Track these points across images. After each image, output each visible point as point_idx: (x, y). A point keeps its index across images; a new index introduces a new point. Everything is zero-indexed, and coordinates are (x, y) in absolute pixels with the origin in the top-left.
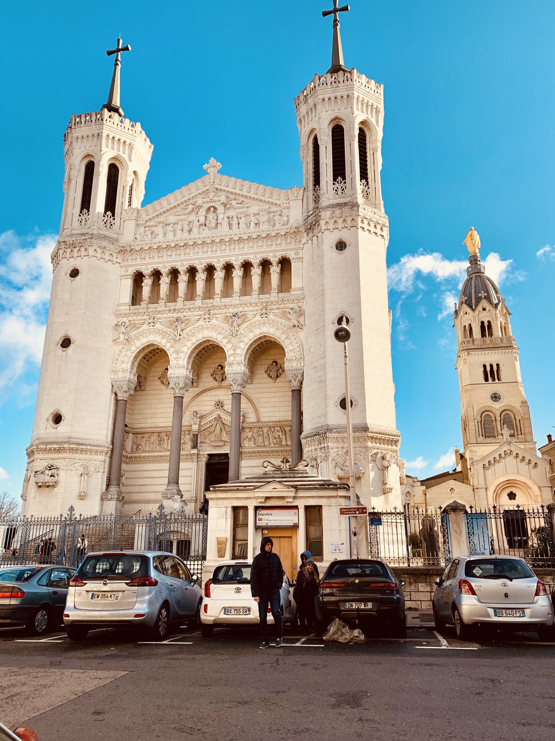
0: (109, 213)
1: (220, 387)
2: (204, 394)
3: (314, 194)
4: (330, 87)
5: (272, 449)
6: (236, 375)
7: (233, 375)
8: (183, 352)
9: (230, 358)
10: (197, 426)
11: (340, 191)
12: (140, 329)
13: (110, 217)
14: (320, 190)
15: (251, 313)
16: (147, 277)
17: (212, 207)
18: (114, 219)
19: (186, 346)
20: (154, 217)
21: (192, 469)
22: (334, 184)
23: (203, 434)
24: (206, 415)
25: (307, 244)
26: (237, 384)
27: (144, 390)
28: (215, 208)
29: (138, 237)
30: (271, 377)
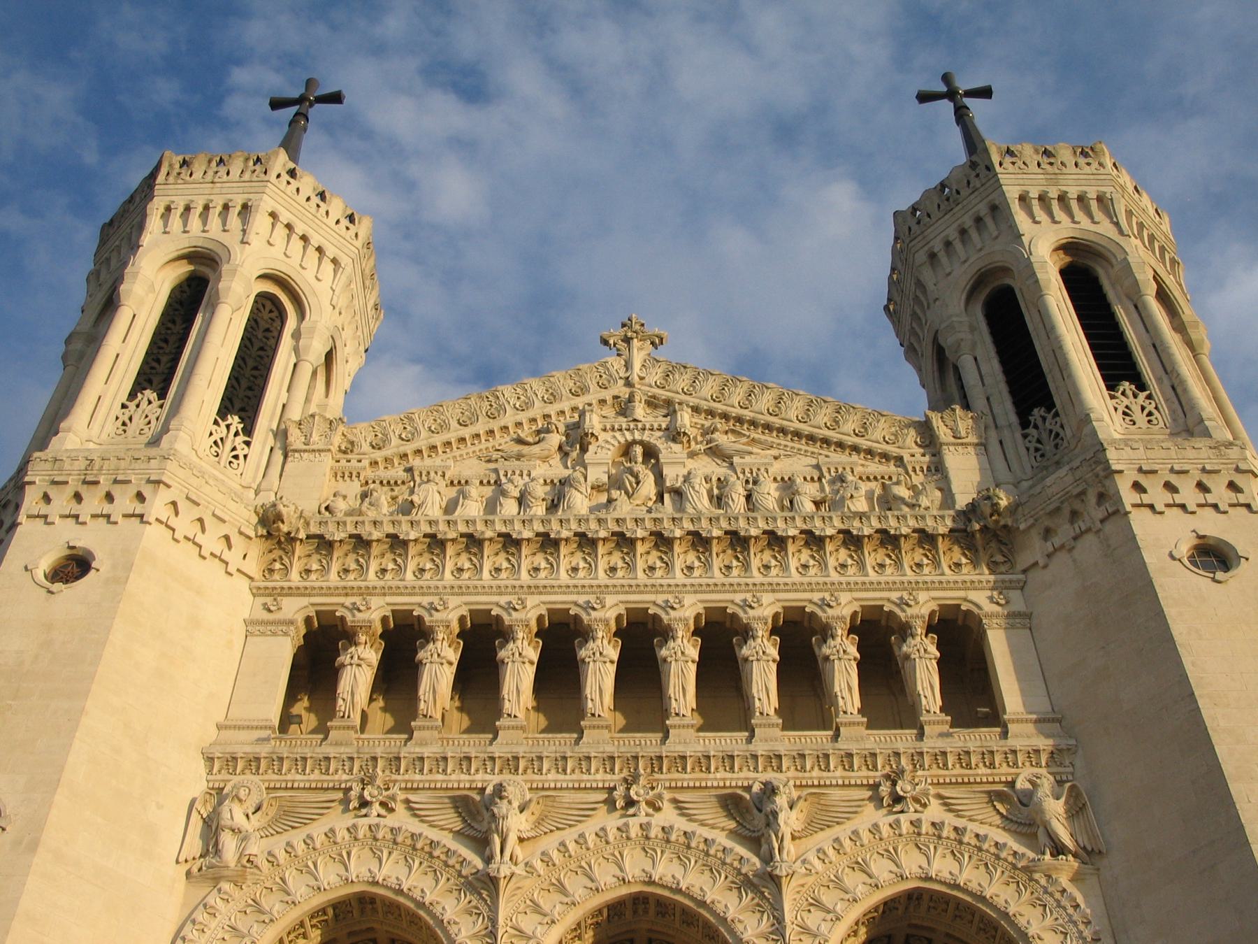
0: (234, 420)
3: (1025, 436)
4: (1040, 171)
11: (1141, 419)
12: (315, 824)
13: (236, 434)
14: (1057, 415)
16: (362, 638)
17: (634, 442)
18: (248, 444)
20: (404, 456)
22: (1112, 397)
25: (1045, 567)
28: (650, 453)
29: (341, 506)
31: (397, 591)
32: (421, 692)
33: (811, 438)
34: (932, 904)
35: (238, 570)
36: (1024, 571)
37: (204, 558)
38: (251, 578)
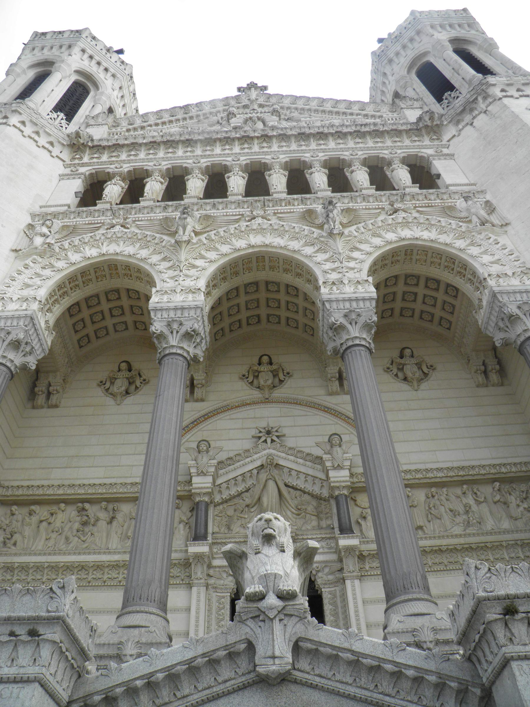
1: (267, 401)
2: (221, 416)
3: (441, 105)
5: (462, 541)
6: (354, 304)
7: (347, 305)
8: (194, 266)
9: (328, 276)
10: (210, 479)
13: (62, 119)
15: (367, 212)
18: (68, 125)
19: (203, 257)
21: (188, 610)
23: (221, 512)
24: (230, 459)
26: (359, 325)
27: (56, 406)
30: (405, 379)
31: (136, 161)
32: (145, 190)
33: (337, 113)
34: (418, 257)
35: (57, 156)
36: (448, 141)
37: (39, 147)
38: (64, 161)
